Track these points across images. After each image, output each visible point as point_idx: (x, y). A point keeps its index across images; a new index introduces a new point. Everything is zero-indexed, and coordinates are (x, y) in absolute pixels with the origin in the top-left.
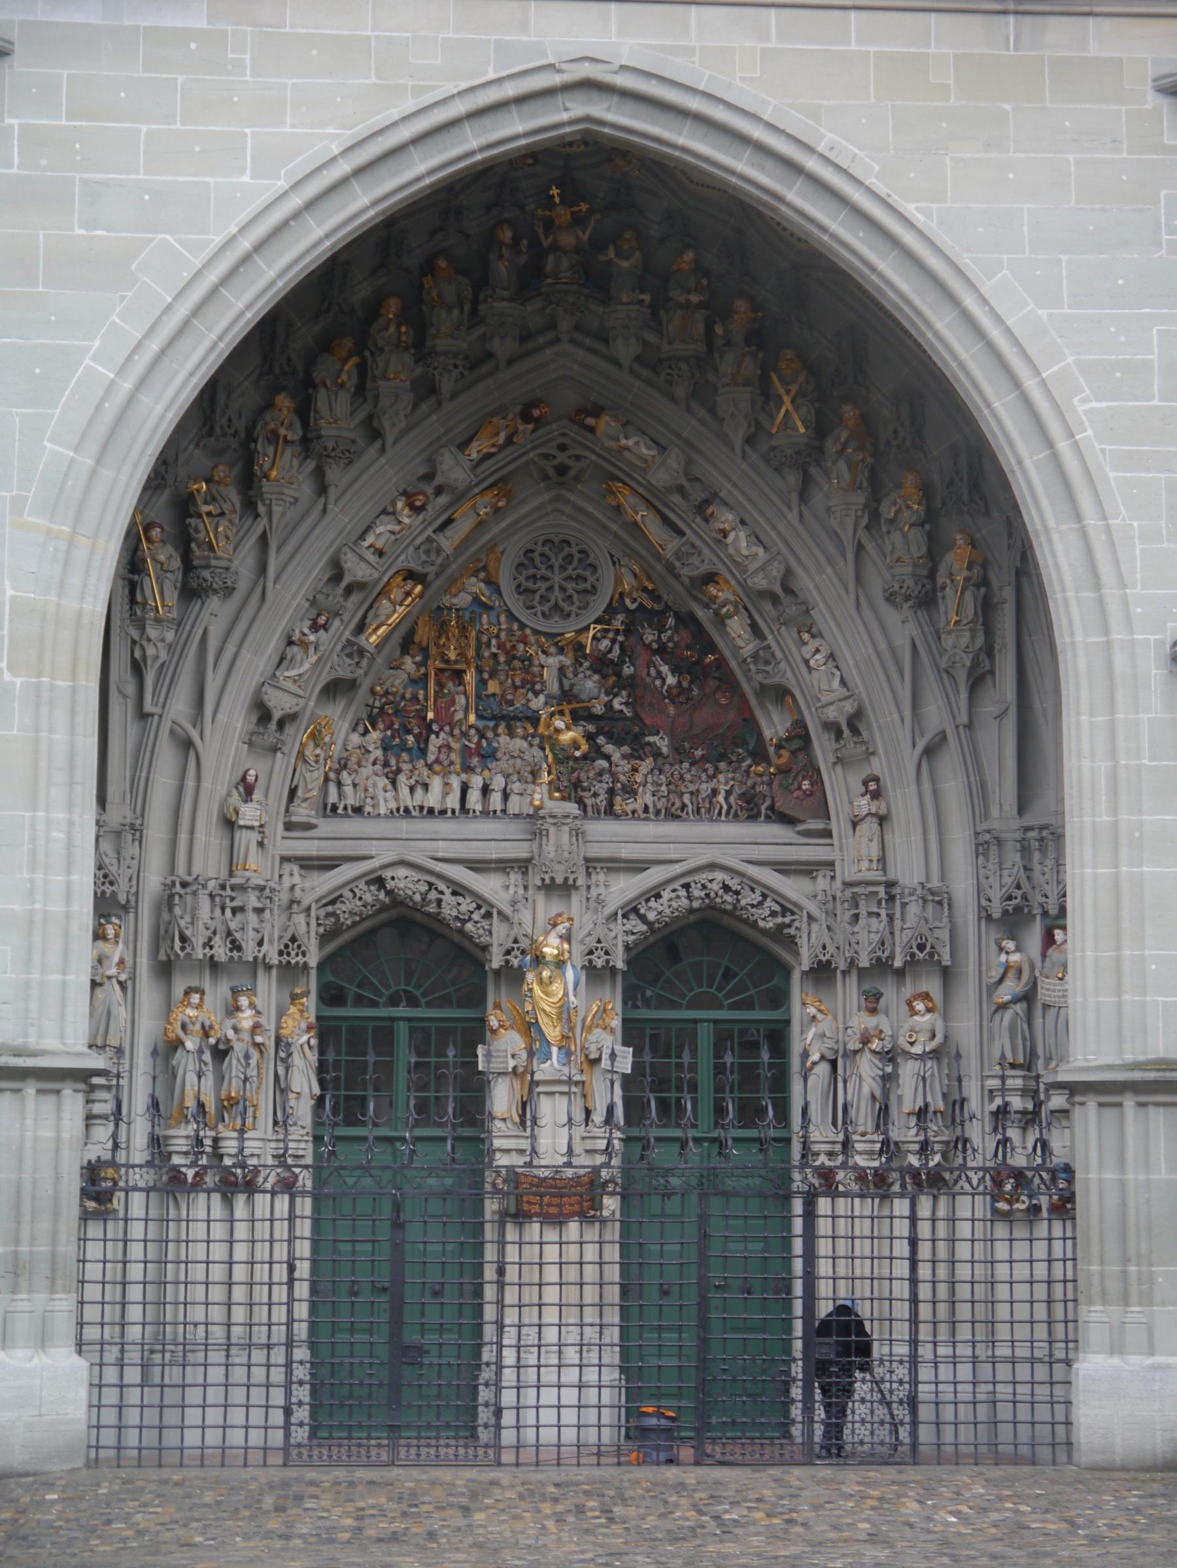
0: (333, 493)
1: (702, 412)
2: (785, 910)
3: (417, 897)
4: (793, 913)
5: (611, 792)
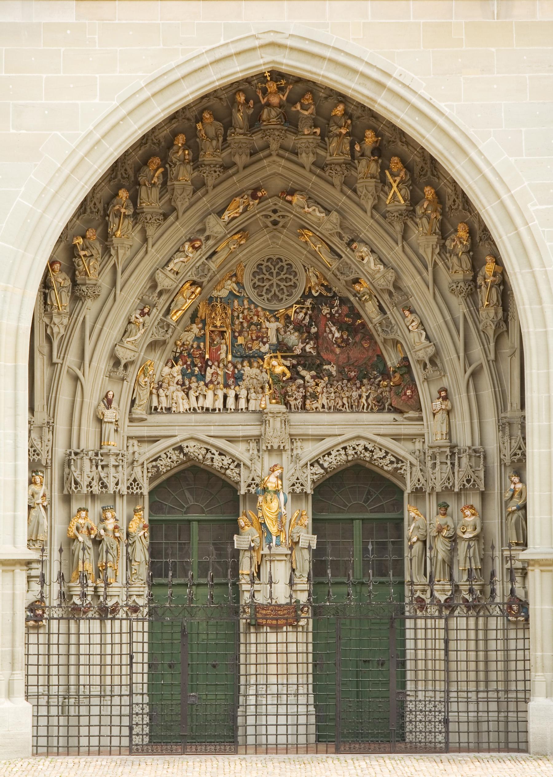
0: (150, 242)
1: (349, 192)
2: (398, 461)
3: (201, 457)
4: (402, 462)
5: (305, 398)
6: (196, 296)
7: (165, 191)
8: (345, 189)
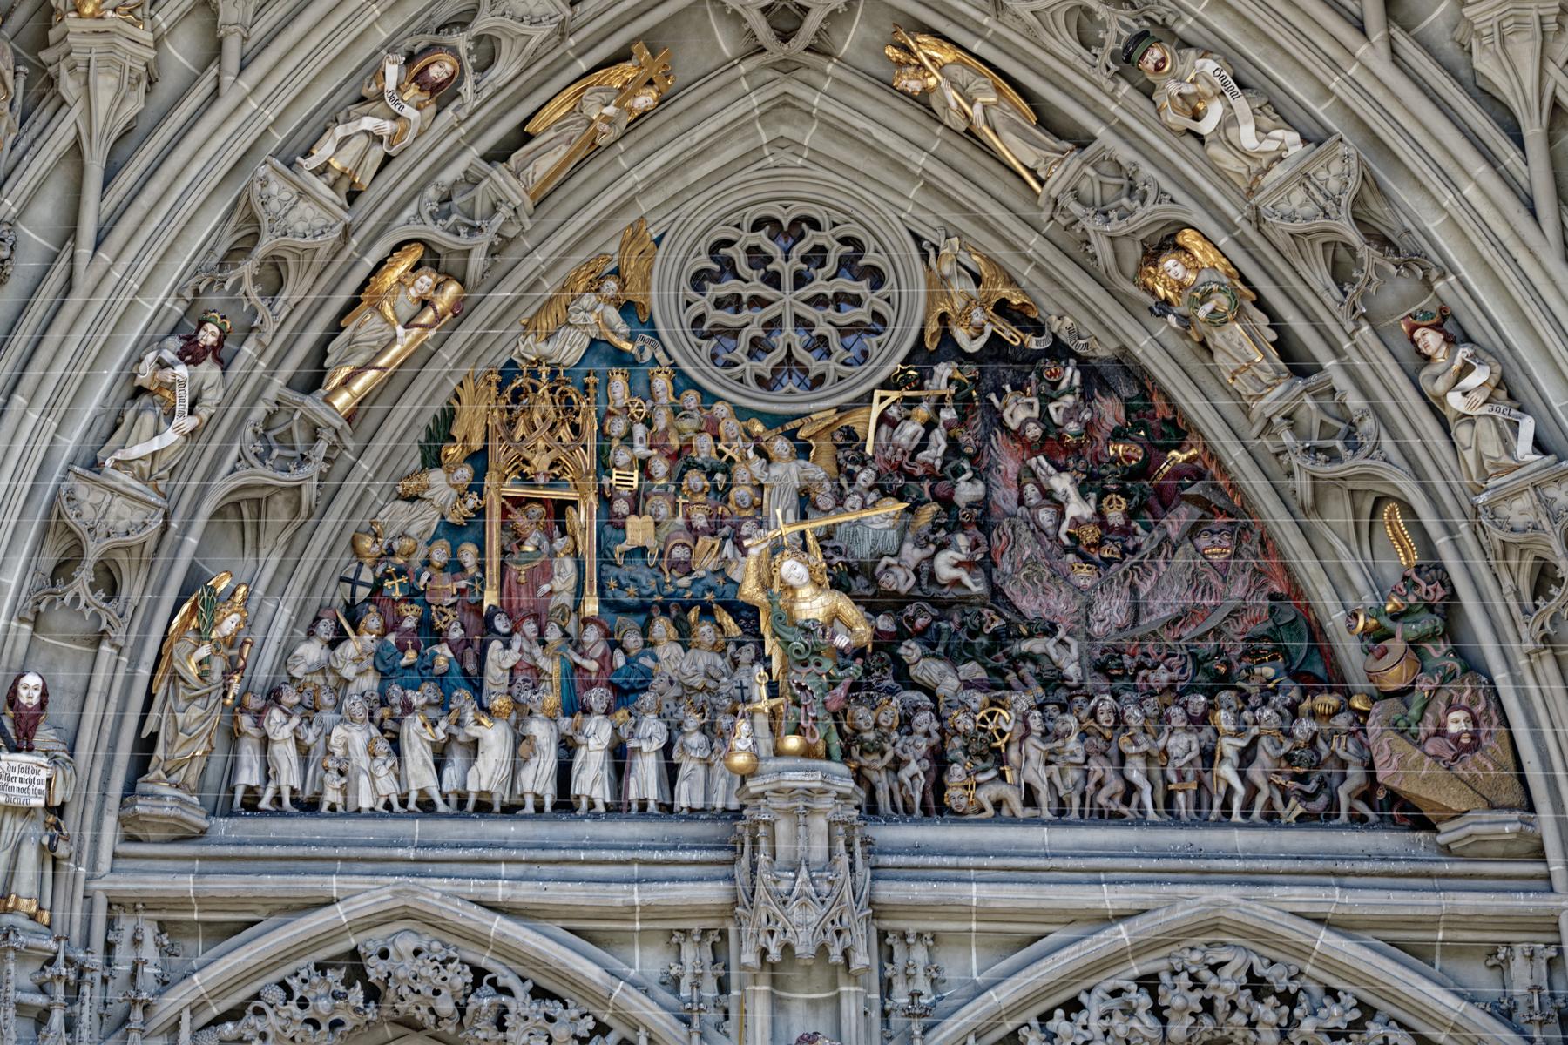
6: (439, 317)
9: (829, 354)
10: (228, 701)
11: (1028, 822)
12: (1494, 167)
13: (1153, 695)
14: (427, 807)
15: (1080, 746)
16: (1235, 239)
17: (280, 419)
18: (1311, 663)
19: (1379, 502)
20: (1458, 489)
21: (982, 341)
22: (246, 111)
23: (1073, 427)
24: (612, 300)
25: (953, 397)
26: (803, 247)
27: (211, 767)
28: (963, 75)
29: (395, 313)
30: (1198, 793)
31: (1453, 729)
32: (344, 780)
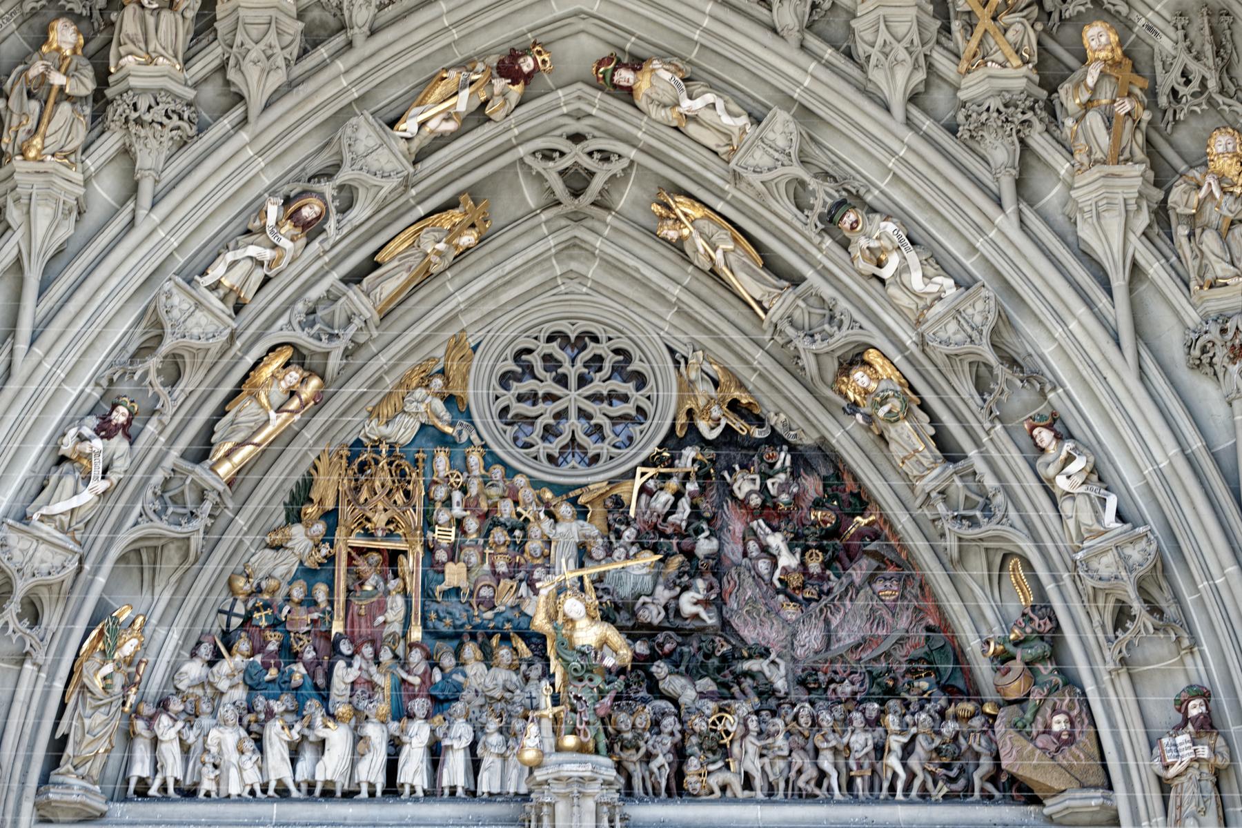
1: (829, 53)
6: (303, 405)
7: (211, 37)
8: (813, 42)
9: (603, 438)
10: (127, 709)
11: (746, 801)
12: (1091, 309)
13: (840, 703)
14: (283, 793)
15: (786, 743)
16: (906, 358)
17: (174, 484)
18: (955, 679)
19: (1006, 557)
20: (1062, 549)
21: (719, 431)
22: (155, 239)
23: (784, 498)
24: (436, 394)
25: (696, 473)
26: (586, 355)
27: (111, 762)
28: (709, 228)
29: (269, 401)
30: (871, 778)
31: (1056, 728)
32: (217, 772)
